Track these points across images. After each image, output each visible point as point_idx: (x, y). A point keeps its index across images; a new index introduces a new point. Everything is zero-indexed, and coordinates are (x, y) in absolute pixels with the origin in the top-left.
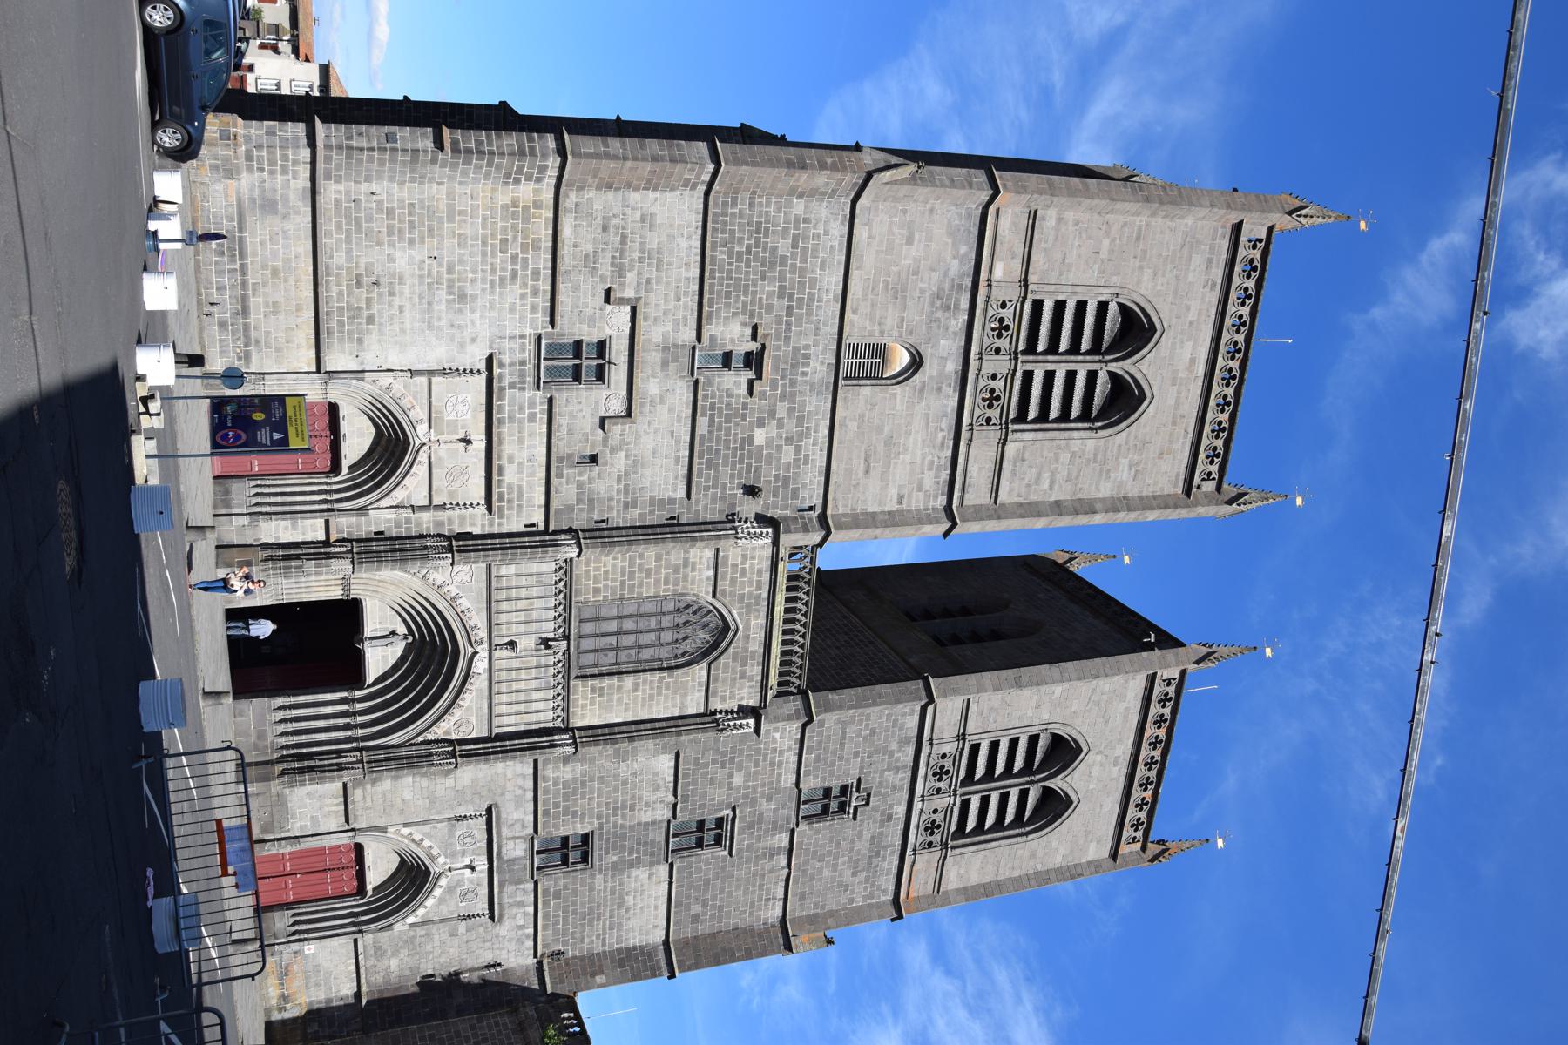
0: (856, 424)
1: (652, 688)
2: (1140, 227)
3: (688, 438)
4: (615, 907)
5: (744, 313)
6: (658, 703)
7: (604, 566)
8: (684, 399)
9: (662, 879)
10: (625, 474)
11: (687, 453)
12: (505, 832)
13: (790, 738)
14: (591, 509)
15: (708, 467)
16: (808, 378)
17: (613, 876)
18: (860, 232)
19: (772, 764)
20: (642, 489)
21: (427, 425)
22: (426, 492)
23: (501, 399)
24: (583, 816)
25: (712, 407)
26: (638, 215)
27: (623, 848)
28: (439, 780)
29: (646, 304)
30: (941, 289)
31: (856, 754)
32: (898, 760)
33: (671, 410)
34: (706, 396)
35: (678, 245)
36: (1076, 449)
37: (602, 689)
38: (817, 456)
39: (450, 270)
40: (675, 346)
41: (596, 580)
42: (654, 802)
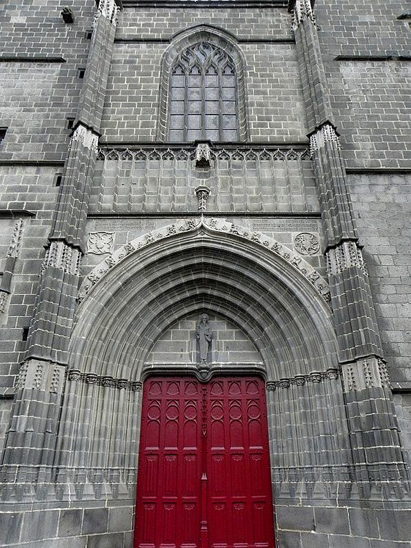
14: (55, 131)
28: (383, 272)
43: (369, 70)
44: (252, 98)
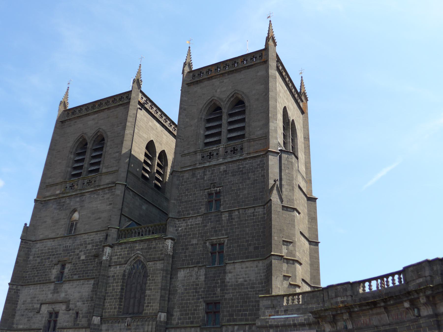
1: (152, 283)
3: (78, 281)
4: (243, 287)
5: (50, 269)
8: (67, 284)
9: (233, 267)
11: (82, 281)
13: (182, 223)
17: (227, 290)
18: (41, 237)
19: (191, 228)
24: (197, 306)
26: (22, 306)
32: (201, 176)
33: (69, 288)
35: (31, 293)
38: (92, 236)
40: (54, 290)
41: (111, 309)
42: (197, 275)
43: (188, 273)
44: (148, 292)
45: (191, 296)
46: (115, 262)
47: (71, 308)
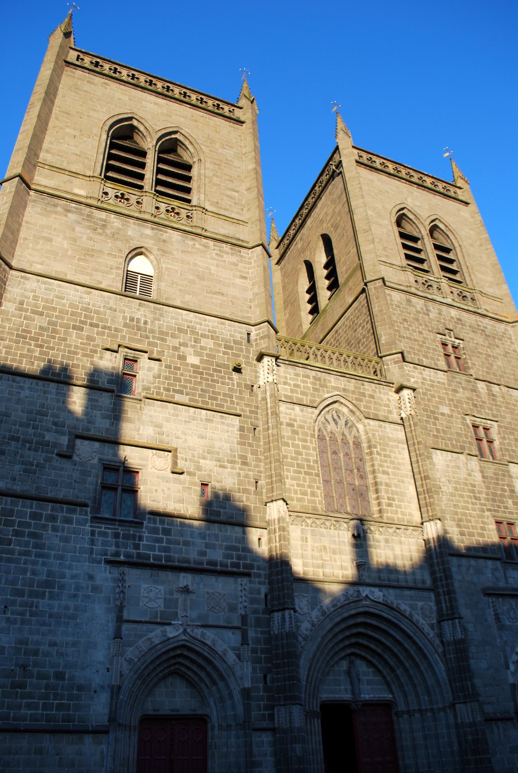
0: (187, 296)
1: (386, 461)
2: (60, 111)
6: (396, 458)
7: (293, 486)
8: (159, 409)
10: (219, 461)
12: (502, 584)
15: (216, 399)
16: (149, 321)
18: (38, 268)
20: (231, 450)
21: (168, 628)
22: (229, 634)
23: (148, 557)
24: (483, 523)
25: (168, 390)
27: (502, 496)
29: (75, 428)
30: (89, 227)
31: (420, 333)
33: (168, 420)
34: (158, 393)
35: (27, 397)
36: (212, 173)
37: (389, 498)
39: (20, 593)
41: (304, 493)
42: (468, 470)
45: (468, 503)
46: (286, 396)
47: (185, 470)
